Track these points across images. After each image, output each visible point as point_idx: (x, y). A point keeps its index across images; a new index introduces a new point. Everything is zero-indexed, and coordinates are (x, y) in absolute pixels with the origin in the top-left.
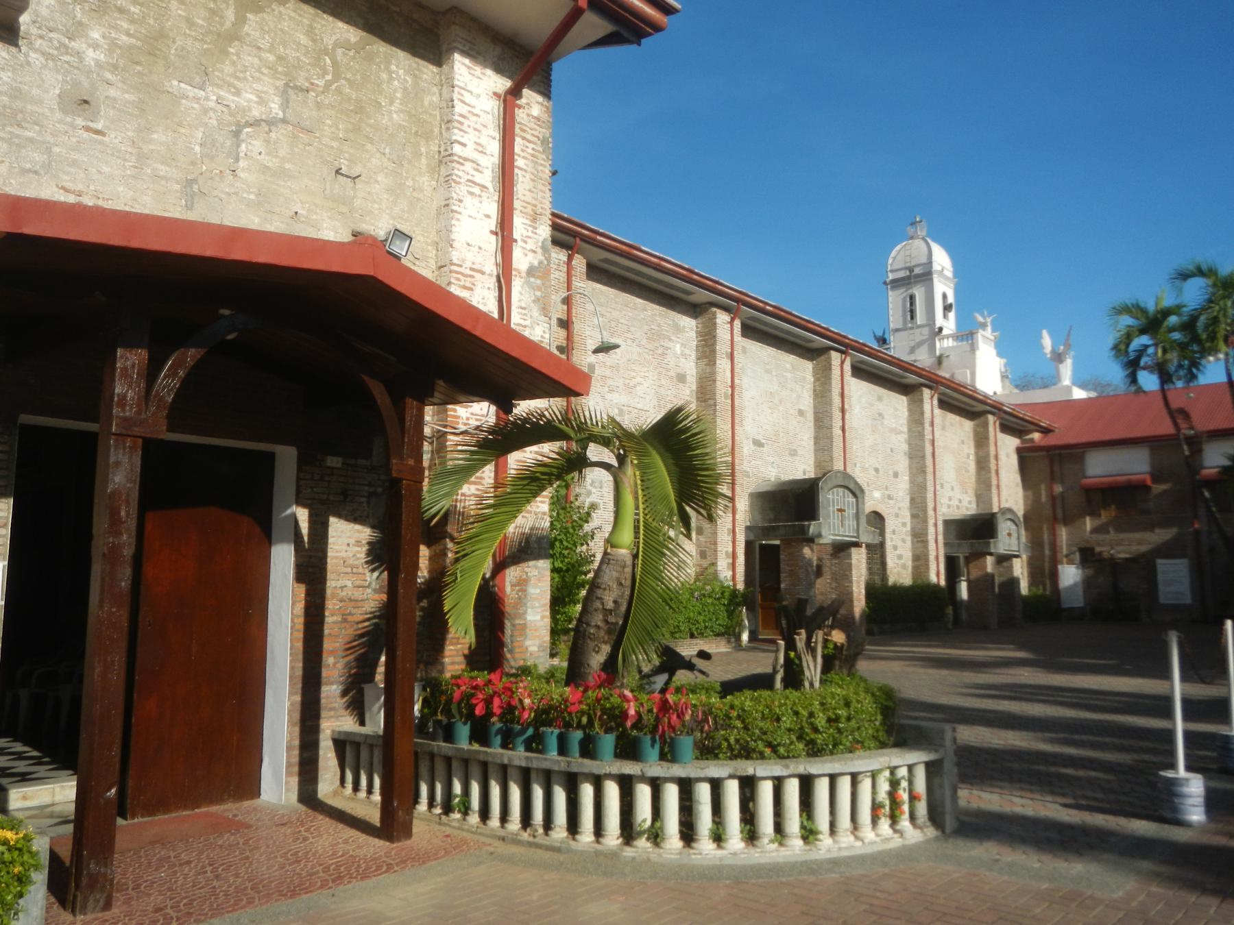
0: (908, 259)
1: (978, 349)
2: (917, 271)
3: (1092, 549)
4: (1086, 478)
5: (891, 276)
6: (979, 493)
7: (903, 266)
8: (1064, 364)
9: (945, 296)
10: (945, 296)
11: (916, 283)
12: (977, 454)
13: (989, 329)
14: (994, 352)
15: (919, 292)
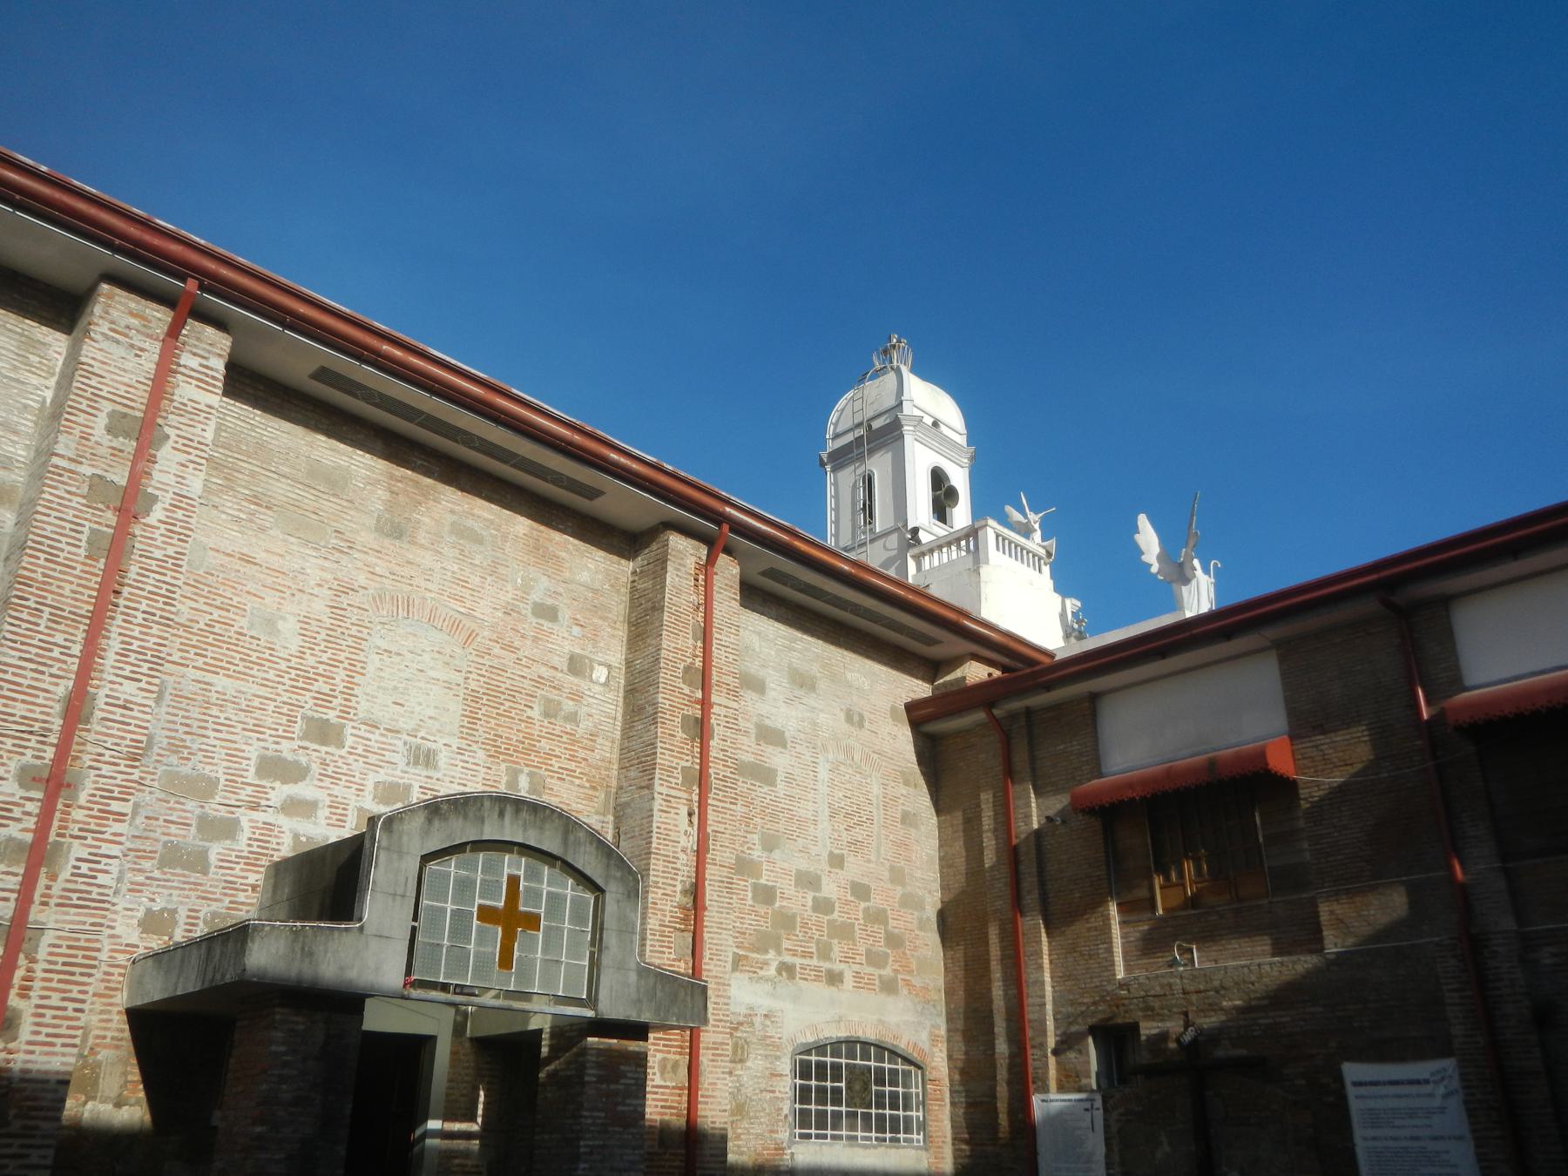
0: (858, 405)
1: (987, 562)
2: (876, 424)
3: (1134, 1028)
4: (1101, 776)
5: (832, 446)
6: (624, 799)
7: (849, 424)
8: (1194, 582)
9: (938, 477)
10: (938, 477)
11: (871, 452)
12: (629, 663)
13: (1037, 536)
14: (1044, 580)
15: (879, 466)
